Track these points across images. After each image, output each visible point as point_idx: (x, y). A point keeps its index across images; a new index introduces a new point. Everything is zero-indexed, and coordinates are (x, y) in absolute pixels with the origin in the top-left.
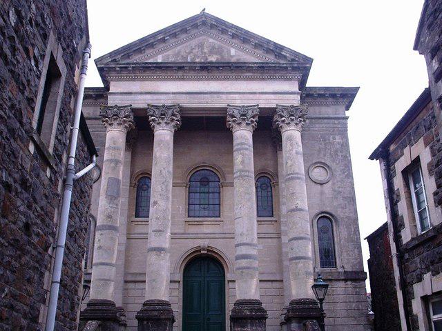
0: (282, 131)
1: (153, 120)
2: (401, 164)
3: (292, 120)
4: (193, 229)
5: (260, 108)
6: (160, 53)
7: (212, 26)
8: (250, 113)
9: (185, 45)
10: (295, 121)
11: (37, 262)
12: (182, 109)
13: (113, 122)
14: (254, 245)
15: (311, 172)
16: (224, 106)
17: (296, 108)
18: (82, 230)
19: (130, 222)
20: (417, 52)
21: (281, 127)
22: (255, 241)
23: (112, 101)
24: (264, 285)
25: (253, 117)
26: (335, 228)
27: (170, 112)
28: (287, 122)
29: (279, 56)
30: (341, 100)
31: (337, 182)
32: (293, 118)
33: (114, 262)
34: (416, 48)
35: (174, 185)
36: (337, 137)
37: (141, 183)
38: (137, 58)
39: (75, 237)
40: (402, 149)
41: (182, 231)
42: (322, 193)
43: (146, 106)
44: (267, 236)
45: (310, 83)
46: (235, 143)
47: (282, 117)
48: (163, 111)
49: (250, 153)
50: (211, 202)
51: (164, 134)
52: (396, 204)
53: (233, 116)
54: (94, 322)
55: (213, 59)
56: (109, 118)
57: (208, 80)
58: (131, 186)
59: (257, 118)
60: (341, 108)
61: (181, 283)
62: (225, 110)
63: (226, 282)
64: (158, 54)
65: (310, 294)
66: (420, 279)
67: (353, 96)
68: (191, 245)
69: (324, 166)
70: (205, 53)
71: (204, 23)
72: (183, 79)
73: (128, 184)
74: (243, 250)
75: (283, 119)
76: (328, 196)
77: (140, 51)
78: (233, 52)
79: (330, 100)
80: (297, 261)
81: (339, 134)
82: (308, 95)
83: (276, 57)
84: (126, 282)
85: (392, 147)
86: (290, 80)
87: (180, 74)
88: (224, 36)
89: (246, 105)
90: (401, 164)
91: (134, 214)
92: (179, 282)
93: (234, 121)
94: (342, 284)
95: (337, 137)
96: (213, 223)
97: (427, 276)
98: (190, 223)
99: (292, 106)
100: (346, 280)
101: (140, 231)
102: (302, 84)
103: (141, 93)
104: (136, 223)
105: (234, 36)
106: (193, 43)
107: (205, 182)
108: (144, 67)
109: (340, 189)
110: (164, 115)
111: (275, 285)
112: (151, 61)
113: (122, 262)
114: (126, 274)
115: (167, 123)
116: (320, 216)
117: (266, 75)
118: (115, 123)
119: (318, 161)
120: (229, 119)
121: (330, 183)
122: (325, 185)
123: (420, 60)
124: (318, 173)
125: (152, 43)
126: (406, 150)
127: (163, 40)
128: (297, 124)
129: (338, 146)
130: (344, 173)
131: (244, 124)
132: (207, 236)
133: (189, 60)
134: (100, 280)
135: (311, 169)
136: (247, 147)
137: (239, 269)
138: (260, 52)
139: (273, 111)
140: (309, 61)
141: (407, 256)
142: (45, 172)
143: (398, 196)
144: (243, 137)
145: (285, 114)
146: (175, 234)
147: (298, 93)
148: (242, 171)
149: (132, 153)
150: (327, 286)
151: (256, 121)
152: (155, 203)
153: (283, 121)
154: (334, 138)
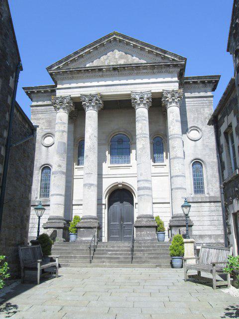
1: (85, 104)
8: (146, 96)
12: (102, 97)
16: (129, 92)
20: (229, 53)
23: (59, 93)
27: (95, 99)
31: (206, 139)
32: (173, 98)
34: (228, 51)
36: (206, 109)
38: (72, 66)
42: (195, 146)
46: (137, 116)
47: (167, 98)
48: (91, 97)
49: (146, 123)
58: (74, 146)
62: (129, 95)
67: (217, 82)
70: (116, 59)
73: (72, 145)
75: (168, 99)
79: (201, 85)
85: (219, 117)
86: (172, 72)
87: (101, 73)
88: (128, 47)
89: (143, 91)
90: (223, 128)
99: (173, 91)
102: (181, 75)
109: (208, 144)
123: (229, 58)
126: (225, 119)
130: (210, 133)
131: (142, 105)
133: (106, 64)
136: (144, 118)
143: (222, 149)
144: (142, 112)
145: (169, 96)
147: (177, 82)
150: (190, 206)
152: (87, 156)
154: (204, 110)
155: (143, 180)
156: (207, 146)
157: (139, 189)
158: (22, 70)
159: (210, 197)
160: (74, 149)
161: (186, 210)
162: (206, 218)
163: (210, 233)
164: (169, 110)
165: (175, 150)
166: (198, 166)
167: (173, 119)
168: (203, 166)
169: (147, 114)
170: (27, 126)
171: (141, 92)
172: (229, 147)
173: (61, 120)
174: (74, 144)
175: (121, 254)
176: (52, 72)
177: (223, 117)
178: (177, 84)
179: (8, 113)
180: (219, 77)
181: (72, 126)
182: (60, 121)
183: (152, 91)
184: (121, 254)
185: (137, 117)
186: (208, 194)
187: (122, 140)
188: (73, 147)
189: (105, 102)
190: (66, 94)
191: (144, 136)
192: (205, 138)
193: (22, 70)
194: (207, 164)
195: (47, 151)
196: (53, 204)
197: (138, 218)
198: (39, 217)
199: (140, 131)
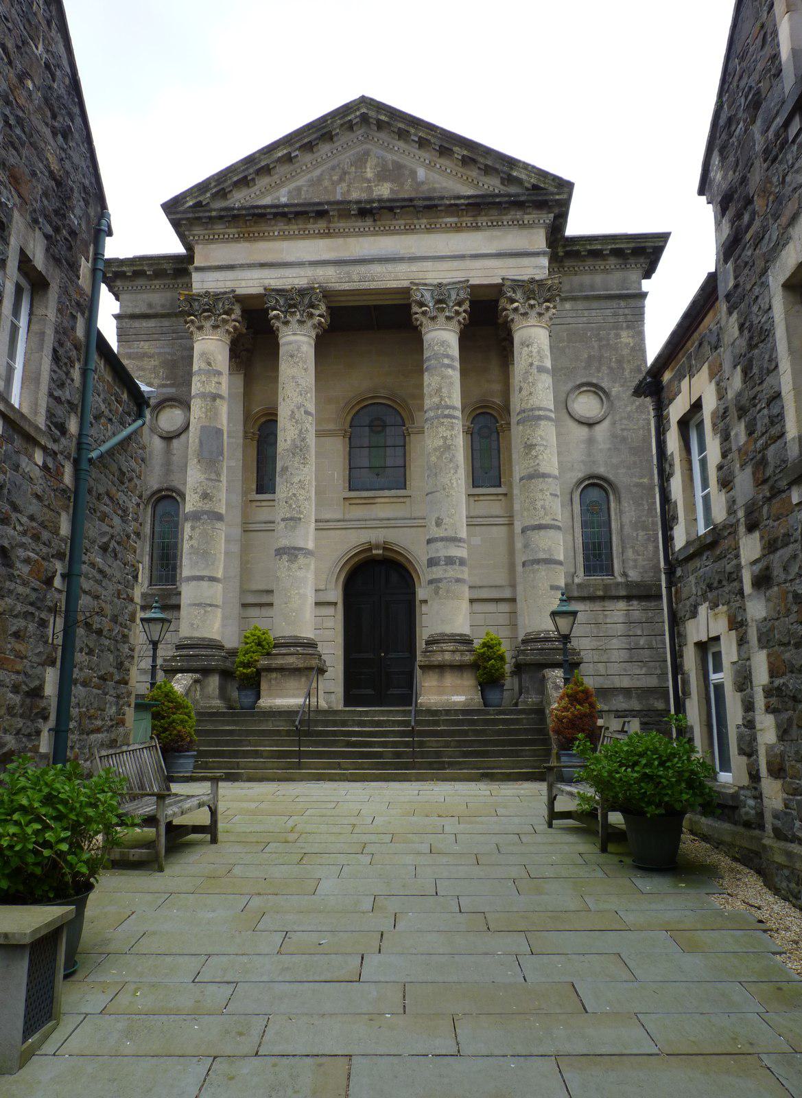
0: (514, 327)
1: (277, 317)
2: (677, 410)
3: (532, 307)
4: (358, 512)
5: (473, 287)
7: (380, 125)
10: (537, 309)
11: (32, 604)
12: (327, 294)
13: (204, 323)
14: (460, 540)
15: (573, 401)
16: (406, 284)
17: (540, 283)
18: (128, 537)
19: (248, 503)
20: (704, 198)
21: (512, 320)
22: (463, 534)
23: (202, 283)
24: (478, 607)
25: (460, 304)
26: (613, 505)
27: (306, 301)
28: (522, 311)
29: (509, 180)
30: (632, 260)
32: (532, 302)
33: (220, 575)
34: (701, 192)
35: (320, 434)
36: (624, 334)
38: (239, 198)
39: (114, 550)
40: (680, 381)
41: (340, 516)
42: (591, 441)
43: (261, 290)
44: (492, 521)
45: (575, 227)
46: (427, 354)
47: (513, 301)
48: (296, 300)
49: (455, 375)
50: (389, 462)
52: (668, 480)
53: (421, 304)
55: (384, 191)
56: (195, 316)
57: (375, 234)
58: (245, 437)
59: (466, 306)
60: (633, 275)
61: (340, 606)
62: (406, 292)
63: (417, 603)
64: (278, 186)
65: (546, 625)
66: (694, 614)
68: (354, 540)
69: (597, 389)
70: (369, 181)
71: (365, 119)
73: (241, 434)
74: (443, 551)
75: (516, 304)
76: (602, 446)
77: (245, 182)
78: (421, 173)
79: (612, 261)
80: (536, 567)
81: (628, 327)
82: (569, 254)
83: (502, 183)
84: (244, 606)
85: (667, 376)
86: (530, 226)
87: (321, 225)
89: (444, 281)
90: (677, 410)
91: (254, 487)
92: (336, 604)
93: (424, 313)
94: (622, 605)
95: (624, 334)
96: (392, 500)
97: (703, 610)
99: (532, 281)
100: (628, 598)
101: (263, 518)
104: (258, 504)
105: (422, 143)
106: (346, 157)
108: (254, 215)
109: (625, 433)
110: (294, 306)
111: (504, 607)
112: (267, 201)
114: (243, 591)
115: (301, 322)
116: (586, 483)
117: (482, 220)
118: (208, 325)
119: (584, 380)
120: (415, 309)
121: (606, 424)
122: (598, 428)
124: (586, 405)
125: (268, 165)
126: (685, 384)
127: (289, 159)
128: (540, 315)
129: (626, 352)
131: (441, 319)
132: (387, 523)
133: (339, 197)
134: (195, 605)
135: (572, 396)
136: (446, 361)
137: (431, 582)
138: (474, 173)
139: (498, 289)
140: (565, 187)
141: (679, 572)
142: (31, 458)
143: (671, 465)
144: (443, 343)
145: (519, 295)
146: (328, 521)
149: (245, 375)
150: (574, 614)
151: (465, 311)
152: (285, 469)
153: (516, 310)
154: (618, 336)
155: (442, 539)
156: (624, 439)
157: (432, 562)
158: (110, 234)
159: (628, 585)
160: (245, 447)
161: (563, 623)
162: (615, 643)
163: (626, 683)
164: (518, 337)
165: (534, 453)
166: (595, 494)
167: (531, 364)
168: (612, 497)
169: (455, 351)
170: (125, 396)
171: (440, 285)
172: (690, 462)
173: (209, 364)
174: (245, 432)
175: (384, 744)
176: (179, 216)
177: (680, 377)
178: (545, 261)
179: (77, 366)
180: (664, 238)
181: (239, 380)
182: (203, 366)
183: (473, 282)
184: (384, 744)
185: (429, 359)
186: (625, 575)
188: (241, 441)
189: (334, 311)
190: (221, 284)
191: (446, 412)
192: (617, 417)
193: (110, 234)
194: (623, 491)
195: (168, 452)
197: (428, 643)
199: (436, 400)
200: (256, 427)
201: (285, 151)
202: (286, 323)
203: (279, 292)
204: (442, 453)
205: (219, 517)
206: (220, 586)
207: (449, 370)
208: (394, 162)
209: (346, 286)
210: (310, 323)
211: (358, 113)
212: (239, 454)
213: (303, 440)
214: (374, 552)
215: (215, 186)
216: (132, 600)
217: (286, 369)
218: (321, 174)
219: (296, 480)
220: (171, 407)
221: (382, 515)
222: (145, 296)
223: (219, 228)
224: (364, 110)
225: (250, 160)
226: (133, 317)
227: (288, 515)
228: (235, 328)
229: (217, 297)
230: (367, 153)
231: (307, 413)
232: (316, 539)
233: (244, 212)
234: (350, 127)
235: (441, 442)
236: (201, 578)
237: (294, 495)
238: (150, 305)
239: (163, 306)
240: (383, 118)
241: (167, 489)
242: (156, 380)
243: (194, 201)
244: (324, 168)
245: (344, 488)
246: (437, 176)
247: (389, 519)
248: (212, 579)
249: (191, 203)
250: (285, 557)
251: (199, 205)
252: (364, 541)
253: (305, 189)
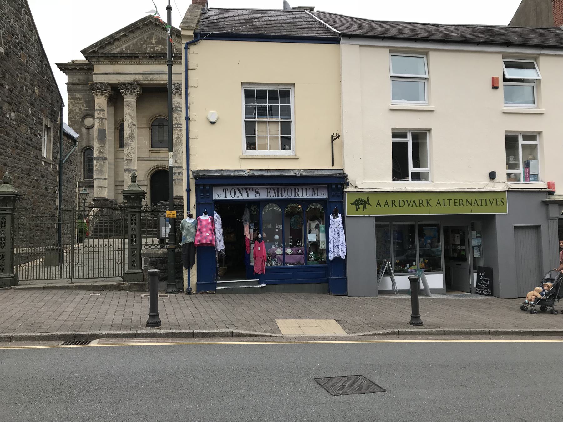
1: (123, 92)
4: (154, 155)
6: (124, 44)
9: (140, 37)
11: (52, 197)
12: (139, 84)
13: (98, 93)
18: (73, 176)
19: (116, 152)
33: (106, 177)
37: (120, 127)
39: (70, 181)
41: (148, 157)
43: (117, 82)
51: (130, 99)
54: (96, 209)
56: (95, 91)
58: (115, 129)
61: (149, 186)
64: (122, 45)
68: (153, 164)
70: (153, 44)
71: (151, 22)
72: (139, 63)
73: (113, 128)
77: (109, 43)
84: (116, 186)
87: (137, 60)
92: (147, 185)
98: (152, 152)
103: (114, 73)
104: (120, 152)
106: (146, 35)
107: (161, 126)
108: (113, 56)
110: (128, 89)
113: (113, 174)
114: (116, 181)
115: (131, 94)
118: (99, 94)
125: (118, 38)
127: (124, 36)
134: (98, 187)
142: (50, 167)
148: (176, 124)
149: (114, 107)
158: (64, 106)
173: (100, 108)
174: (115, 127)
181: (112, 110)
182: (98, 108)
187: (163, 124)
190: (103, 79)
191: (179, 126)
193: (64, 106)
195: (88, 133)
196: (96, 187)
198: (85, 200)
199: (176, 122)
200: (119, 125)
201: (123, 33)
202: (126, 94)
203: (123, 83)
204: (177, 139)
205: (106, 159)
206: (107, 181)
207: (180, 112)
208: (162, 38)
209: (146, 82)
210: (134, 94)
211: (149, 21)
212: (113, 135)
213: (132, 134)
214: (160, 168)
215: (99, 45)
216: (76, 192)
217: (127, 110)
218: (137, 41)
219: (130, 147)
220: (89, 117)
221: (162, 156)
222: (77, 76)
223: (102, 59)
224: (151, 20)
225: (111, 36)
226: (73, 84)
227: (128, 159)
228: (109, 94)
229: (102, 84)
230: (153, 34)
231: (134, 125)
232: (138, 166)
233: (110, 55)
234: (146, 25)
235: (177, 136)
236: (99, 179)
237: (130, 152)
238: (79, 80)
239: (84, 80)
240: (157, 23)
241: (89, 146)
242: (83, 108)
243: (92, 50)
244: (138, 38)
245: (149, 147)
246: (177, 44)
247: (164, 158)
248: (105, 179)
249: (91, 51)
250: (127, 172)
251: (94, 51)
252: (156, 165)
253: (132, 46)
